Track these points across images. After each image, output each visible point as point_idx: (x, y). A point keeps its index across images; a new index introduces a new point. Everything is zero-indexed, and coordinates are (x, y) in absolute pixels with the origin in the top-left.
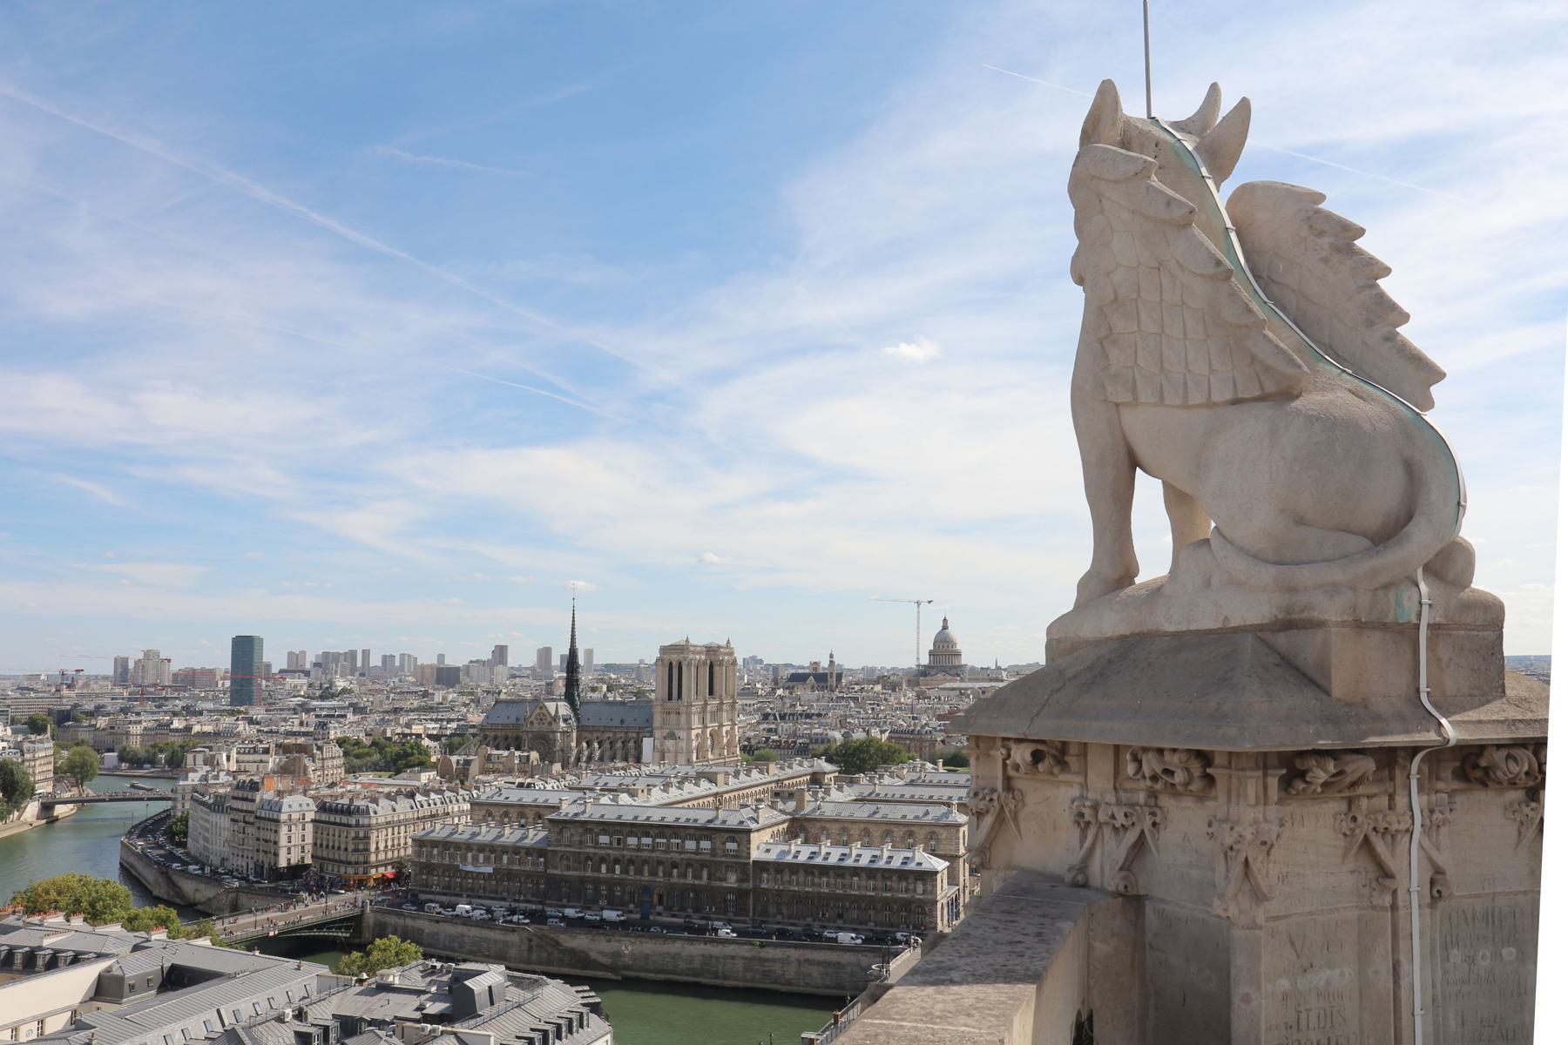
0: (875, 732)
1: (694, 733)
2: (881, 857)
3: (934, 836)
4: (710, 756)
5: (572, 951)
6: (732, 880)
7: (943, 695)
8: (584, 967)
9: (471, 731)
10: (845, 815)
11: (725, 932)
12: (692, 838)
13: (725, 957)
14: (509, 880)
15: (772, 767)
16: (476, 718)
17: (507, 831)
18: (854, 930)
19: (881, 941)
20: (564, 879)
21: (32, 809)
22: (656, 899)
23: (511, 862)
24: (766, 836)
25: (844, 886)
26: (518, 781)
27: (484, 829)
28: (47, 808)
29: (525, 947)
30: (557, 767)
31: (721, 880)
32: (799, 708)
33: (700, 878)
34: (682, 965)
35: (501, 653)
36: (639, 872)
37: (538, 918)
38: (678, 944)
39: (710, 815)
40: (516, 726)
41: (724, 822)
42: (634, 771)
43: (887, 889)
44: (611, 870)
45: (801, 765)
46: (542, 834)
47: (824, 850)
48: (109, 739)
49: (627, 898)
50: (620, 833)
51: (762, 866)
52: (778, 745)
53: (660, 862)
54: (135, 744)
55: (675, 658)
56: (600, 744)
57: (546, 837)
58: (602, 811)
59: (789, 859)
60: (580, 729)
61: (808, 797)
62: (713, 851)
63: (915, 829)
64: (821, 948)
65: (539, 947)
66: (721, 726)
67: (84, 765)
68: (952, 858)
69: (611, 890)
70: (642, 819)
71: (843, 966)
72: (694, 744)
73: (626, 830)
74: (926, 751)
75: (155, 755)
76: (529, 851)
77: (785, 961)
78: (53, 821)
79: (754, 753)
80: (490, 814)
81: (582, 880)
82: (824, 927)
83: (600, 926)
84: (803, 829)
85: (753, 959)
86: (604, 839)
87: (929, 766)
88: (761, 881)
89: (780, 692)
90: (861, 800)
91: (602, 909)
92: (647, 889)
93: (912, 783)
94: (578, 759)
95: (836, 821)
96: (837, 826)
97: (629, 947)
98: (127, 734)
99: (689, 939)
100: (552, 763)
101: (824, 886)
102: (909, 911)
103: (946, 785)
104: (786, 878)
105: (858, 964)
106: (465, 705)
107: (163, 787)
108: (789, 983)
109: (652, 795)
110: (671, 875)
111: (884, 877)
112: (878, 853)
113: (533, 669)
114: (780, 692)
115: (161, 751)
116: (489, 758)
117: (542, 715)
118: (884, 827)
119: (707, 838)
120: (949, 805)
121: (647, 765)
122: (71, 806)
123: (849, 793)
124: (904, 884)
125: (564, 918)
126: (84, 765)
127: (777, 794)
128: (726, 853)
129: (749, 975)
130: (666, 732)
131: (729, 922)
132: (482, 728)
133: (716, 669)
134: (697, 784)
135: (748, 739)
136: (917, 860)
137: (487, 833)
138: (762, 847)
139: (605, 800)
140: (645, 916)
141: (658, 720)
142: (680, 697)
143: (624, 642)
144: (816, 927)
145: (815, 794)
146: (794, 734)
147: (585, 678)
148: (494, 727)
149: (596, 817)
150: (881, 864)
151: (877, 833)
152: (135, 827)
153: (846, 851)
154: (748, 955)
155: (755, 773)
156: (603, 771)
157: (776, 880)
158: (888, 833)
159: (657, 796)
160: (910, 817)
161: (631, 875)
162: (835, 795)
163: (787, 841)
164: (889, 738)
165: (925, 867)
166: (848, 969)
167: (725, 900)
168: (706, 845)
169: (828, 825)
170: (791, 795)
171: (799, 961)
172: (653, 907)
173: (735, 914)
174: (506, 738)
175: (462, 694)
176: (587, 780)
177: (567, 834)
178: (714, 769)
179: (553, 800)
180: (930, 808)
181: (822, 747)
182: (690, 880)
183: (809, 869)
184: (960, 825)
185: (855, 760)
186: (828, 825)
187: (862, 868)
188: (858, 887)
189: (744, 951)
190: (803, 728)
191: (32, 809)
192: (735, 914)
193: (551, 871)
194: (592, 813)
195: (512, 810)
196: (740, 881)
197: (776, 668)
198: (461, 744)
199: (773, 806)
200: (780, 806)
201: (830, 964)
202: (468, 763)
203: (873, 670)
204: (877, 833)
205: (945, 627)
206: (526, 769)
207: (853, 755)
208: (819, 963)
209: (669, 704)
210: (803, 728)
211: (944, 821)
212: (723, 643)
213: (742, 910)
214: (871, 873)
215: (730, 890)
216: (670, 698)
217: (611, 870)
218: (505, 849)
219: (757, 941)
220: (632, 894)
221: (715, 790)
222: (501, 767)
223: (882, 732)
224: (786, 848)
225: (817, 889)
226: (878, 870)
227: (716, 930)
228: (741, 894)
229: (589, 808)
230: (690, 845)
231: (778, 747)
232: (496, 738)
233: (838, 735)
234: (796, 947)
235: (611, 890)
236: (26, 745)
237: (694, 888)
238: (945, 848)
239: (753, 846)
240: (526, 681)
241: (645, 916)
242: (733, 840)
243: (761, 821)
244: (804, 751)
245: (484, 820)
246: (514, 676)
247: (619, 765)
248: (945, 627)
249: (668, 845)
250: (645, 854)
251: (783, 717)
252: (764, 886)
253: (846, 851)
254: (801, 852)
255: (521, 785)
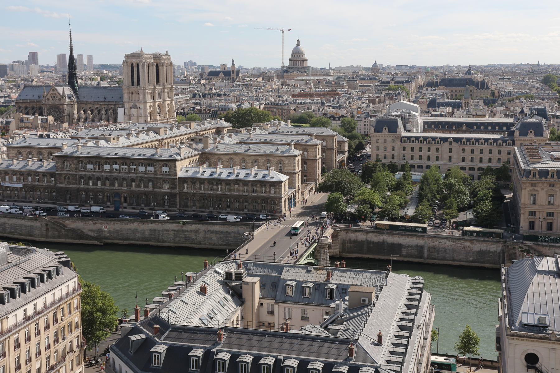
0: (256, 105)
1: (148, 105)
2: (251, 174)
3: (281, 162)
4: (158, 118)
5: (73, 230)
6: (166, 188)
7: (297, 84)
8: (80, 239)
9: (14, 103)
10: (231, 151)
11: (163, 217)
12: (142, 165)
13: (163, 230)
14: (33, 191)
15: (193, 124)
16: (14, 96)
17: (30, 163)
18: (236, 214)
19: (251, 219)
20: (69, 190)
22: (123, 200)
23: (33, 180)
24: (186, 163)
25: (230, 190)
26: (39, 133)
27: (15, 162)
29: (44, 228)
30: (65, 125)
31: (160, 188)
32: (214, 91)
33: (148, 187)
34: (139, 235)
35: (33, 57)
36: (112, 184)
37: (51, 212)
38: (136, 224)
39: (152, 152)
40: (38, 101)
41: (161, 156)
42: (112, 127)
43: (254, 191)
44: (95, 184)
45: (210, 123)
46: (52, 164)
47: (219, 171)
49: (105, 199)
50: (100, 162)
51: (183, 180)
52: (200, 112)
53: (124, 179)
55: (134, 61)
56: (92, 111)
57: (55, 166)
58: (88, 150)
59: (199, 175)
60: (79, 103)
61: (210, 141)
62: (155, 172)
63: (271, 158)
64: (217, 224)
65: (53, 228)
66: (164, 101)
68: (291, 174)
69: (96, 195)
70: (112, 155)
71: (230, 233)
72: (149, 111)
73: (103, 161)
74: (285, 115)
76: (44, 174)
77: (198, 232)
79: (185, 116)
80: (20, 153)
81: (78, 190)
82: (220, 213)
83: (91, 215)
84: (208, 159)
85: (178, 231)
86: (90, 166)
87: (283, 123)
88: (183, 188)
89: (203, 81)
90: (242, 143)
91: (91, 206)
92: (117, 194)
93: (272, 133)
94: (79, 120)
95: (226, 154)
96: (227, 157)
97: (107, 227)
99: (141, 221)
100: (62, 122)
101: (219, 190)
102: (266, 203)
103: (291, 134)
104: (198, 186)
105: (238, 232)
106: (10, 88)
108: (200, 243)
109: (120, 141)
110: (131, 186)
111: (252, 185)
112: (249, 172)
113: (55, 67)
114: (203, 81)
116: (22, 120)
117: (55, 95)
118: (254, 158)
119: (151, 165)
120: (289, 145)
121: (120, 123)
123: (236, 139)
124: (264, 188)
125: (68, 212)
127: (192, 140)
128: (162, 173)
129: (177, 240)
130: (131, 105)
131: (164, 211)
132: (17, 102)
133: (160, 68)
134: (147, 135)
135: (183, 109)
136: (271, 175)
137: (17, 164)
138: (183, 169)
139: (90, 144)
140: (117, 209)
141: (126, 98)
142: (139, 84)
143: (105, 50)
144: (215, 213)
145: (215, 139)
146: (210, 106)
147: (79, 72)
148: (24, 102)
149: (85, 154)
150: (251, 178)
151: (249, 160)
153: (231, 171)
154: (176, 229)
155: (183, 128)
156: (93, 127)
157: (192, 188)
158: (256, 161)
159: (123, 141)
160: (268, 152)
161: (125, 188)
162: (227, 139)
163: (198, 166)
164: (264, 108)
165: (276, 179)
166: (233, 235)
167: (163, 199)
168: (151, 169)
169: (222, 157)
170: (201, 140)
171: (205, 231)
172: (121, 203)
173: (169, 207)
174: (33, 108)
175: (8, 81)
176: (82, 132)
177: (67, 164)
178: (159, 126)
179: (59, 145)
180: (279, 147)
181: (225, 113)
182: (142, 189)
183: (211, 181)
184: (296, 156)
185: (242, 120)
186: (222, 157)
187: (240, 180)
188: (238, 191)
189: (174, 227)
190: (215, 102)
192: (169, 207)
193: (59, 185)
194: (82, 151)
195: (33, 150)
196: (171, 188)
197: (203, 68)
198: (6, 111)
199: (190, 146)
200: (194, 146)
201: (222, 232)
202: (8, 123)
203: (259, 69)
204: (249, 160)
205: (298, 45)
206: (45, 126)
207: (242, 117)
208: (216, 232)
209: (133, 89)
210: (215, 102)
211: (287, 154)
212: (164, 53)
213: (172, 204)
214: (245, 183)
215: (166, 194)
216: (133, 85)
217: (95, 184)
218: (29, 173)
219: (181, 221)
220: (108, 197)
221: (158, 137)
222: (30, 125)
223: (260, 104)
224: (197, 170)
225: (215, 192)
226: (249, 181)
227: (157, 216)
228: (172, 196)
229: (80, 149)
230: (142, 169)
231: (200, 113)
232: (26, 108)
233: (234, 106)
234: (203, 224)
235: (96, 195)
237: (145, 193)
238: (287, 169)
239: (178, 169)
240: (51, 74)
241: (117, 209)
242: (166, 166)
243: (183, 155)
244: (214, 115)
245: (16, 156)
246: (43, 71)
247: (104, 123)
248: (298, 45)
249: (129, 169)
250: (115, 175)
251: (204, 96)
252: (185, 191)
253: (231, 171)
254: (206, 172)
255: (41, 136)
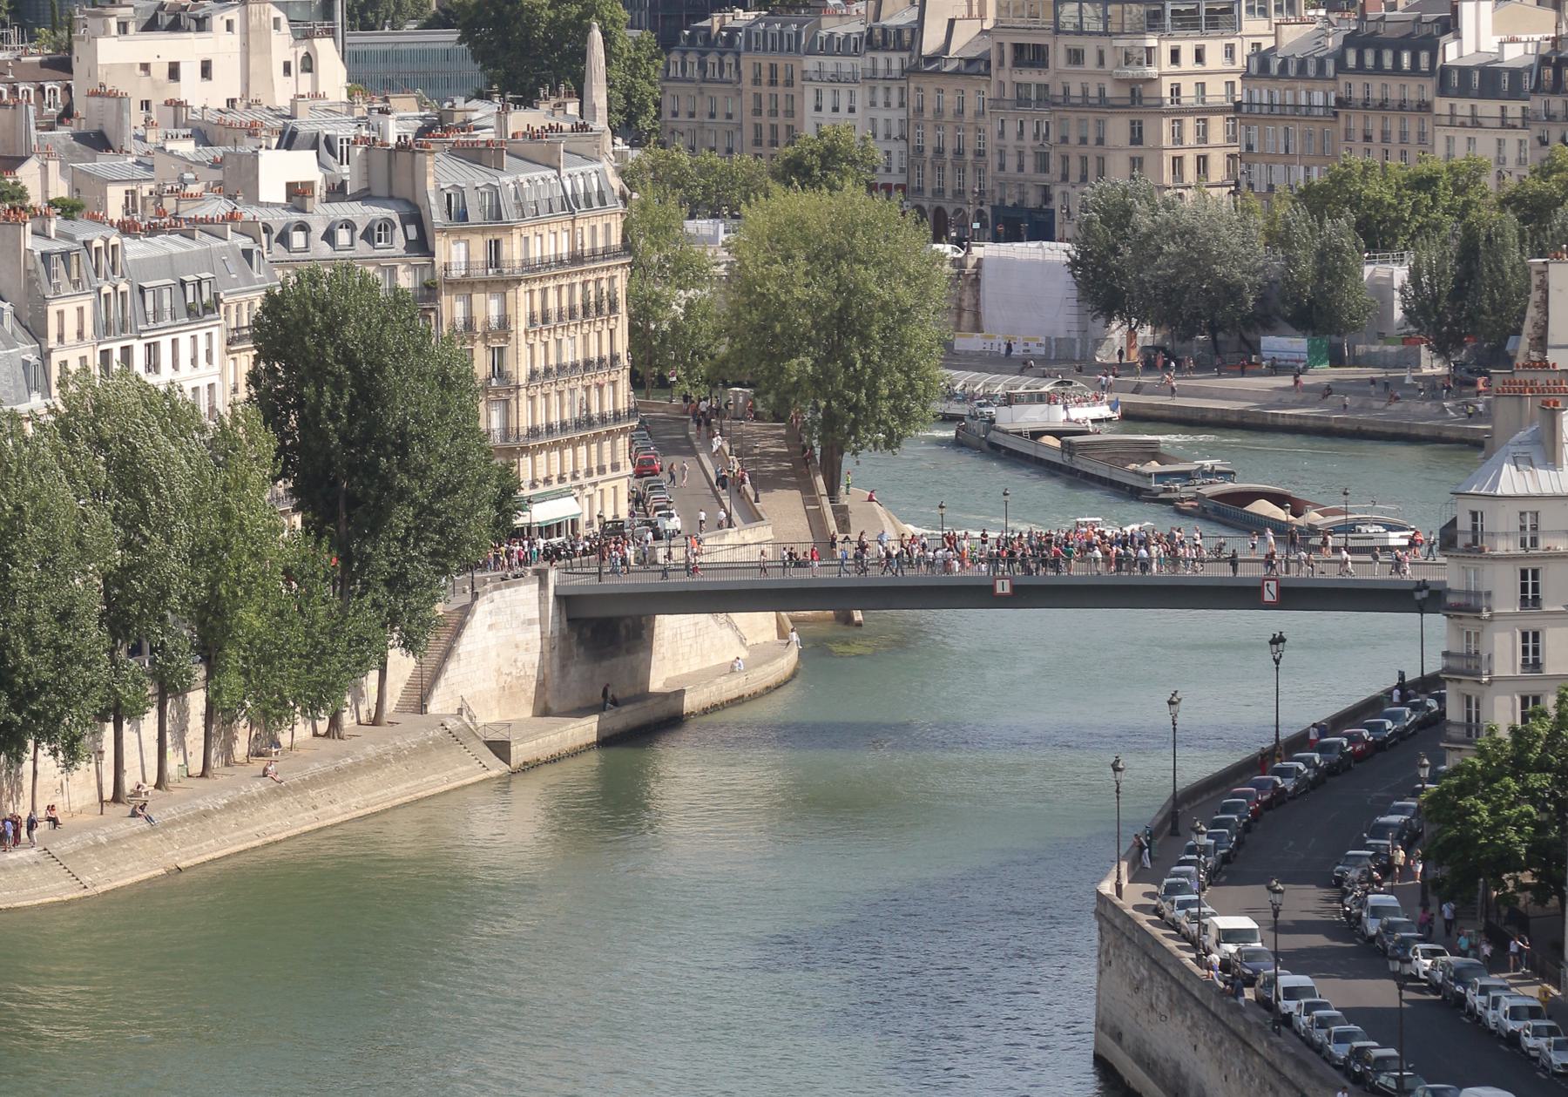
21: (501, 638)
28: (599, 636)
48: (1011, 136)
54: (1196, 178)
67: (843, 324)
75: (1332, 266)
78: (643, 726)
98: (1138, 98)
107: (1385, 509)
115: (1378, 235)
122: (760, 625)
126: (843, 324)
152: (1186, 805)
191: (501, 638)
236: (440, 175)
